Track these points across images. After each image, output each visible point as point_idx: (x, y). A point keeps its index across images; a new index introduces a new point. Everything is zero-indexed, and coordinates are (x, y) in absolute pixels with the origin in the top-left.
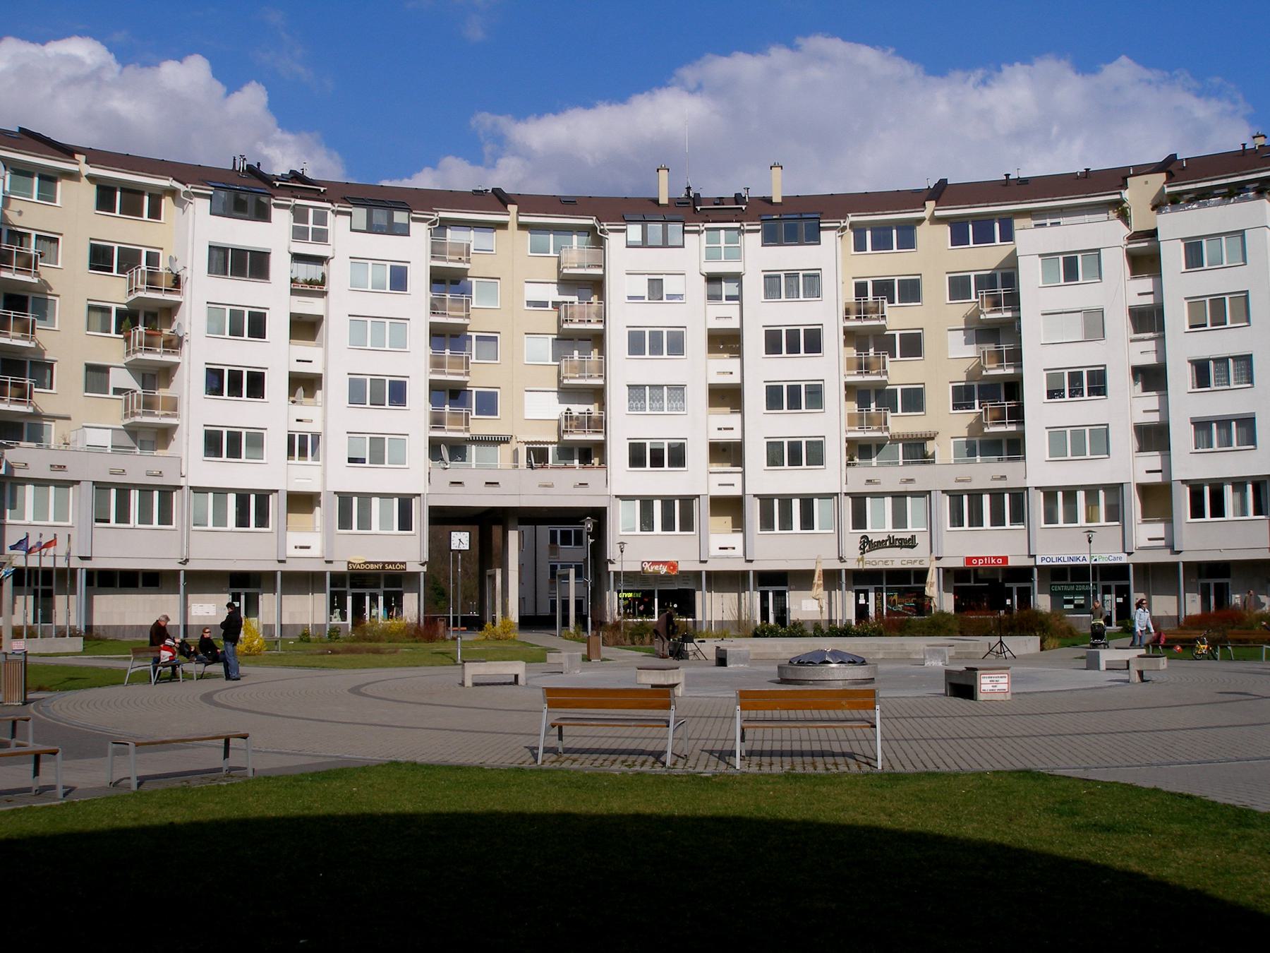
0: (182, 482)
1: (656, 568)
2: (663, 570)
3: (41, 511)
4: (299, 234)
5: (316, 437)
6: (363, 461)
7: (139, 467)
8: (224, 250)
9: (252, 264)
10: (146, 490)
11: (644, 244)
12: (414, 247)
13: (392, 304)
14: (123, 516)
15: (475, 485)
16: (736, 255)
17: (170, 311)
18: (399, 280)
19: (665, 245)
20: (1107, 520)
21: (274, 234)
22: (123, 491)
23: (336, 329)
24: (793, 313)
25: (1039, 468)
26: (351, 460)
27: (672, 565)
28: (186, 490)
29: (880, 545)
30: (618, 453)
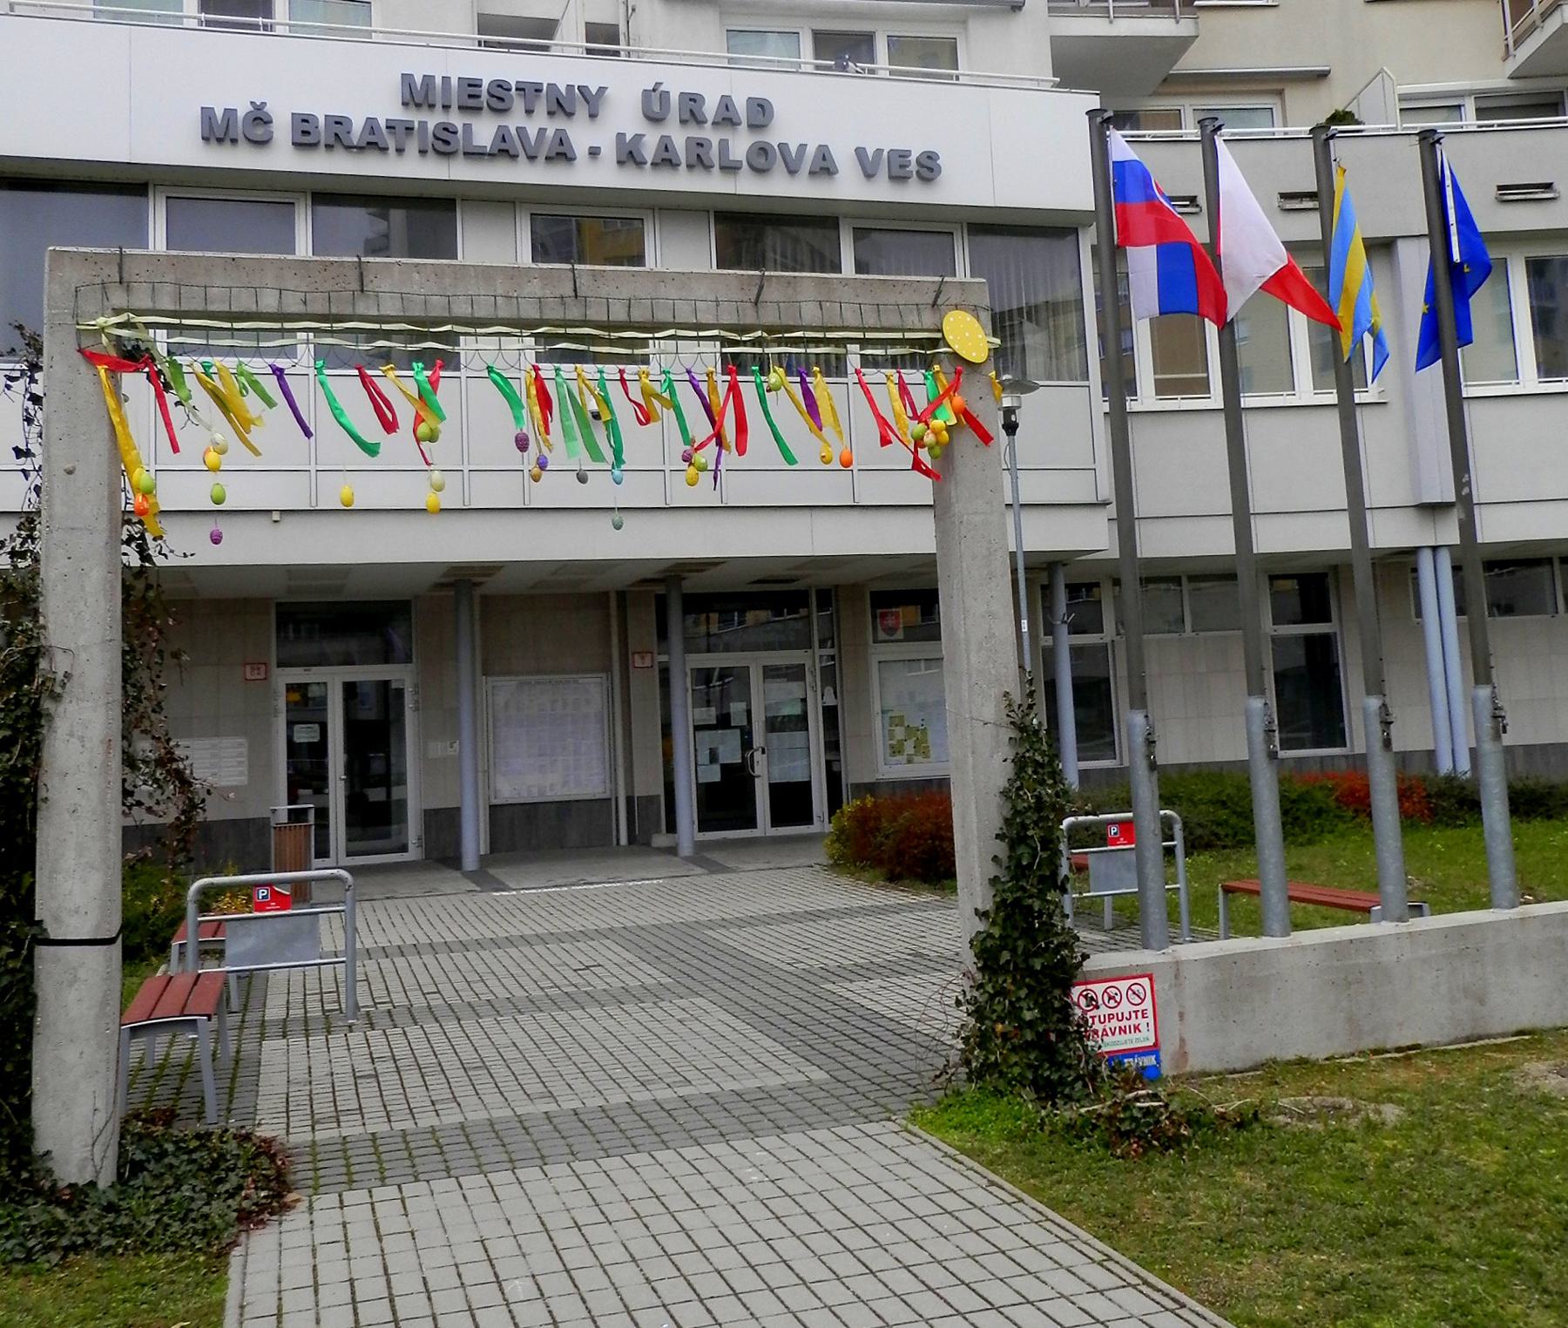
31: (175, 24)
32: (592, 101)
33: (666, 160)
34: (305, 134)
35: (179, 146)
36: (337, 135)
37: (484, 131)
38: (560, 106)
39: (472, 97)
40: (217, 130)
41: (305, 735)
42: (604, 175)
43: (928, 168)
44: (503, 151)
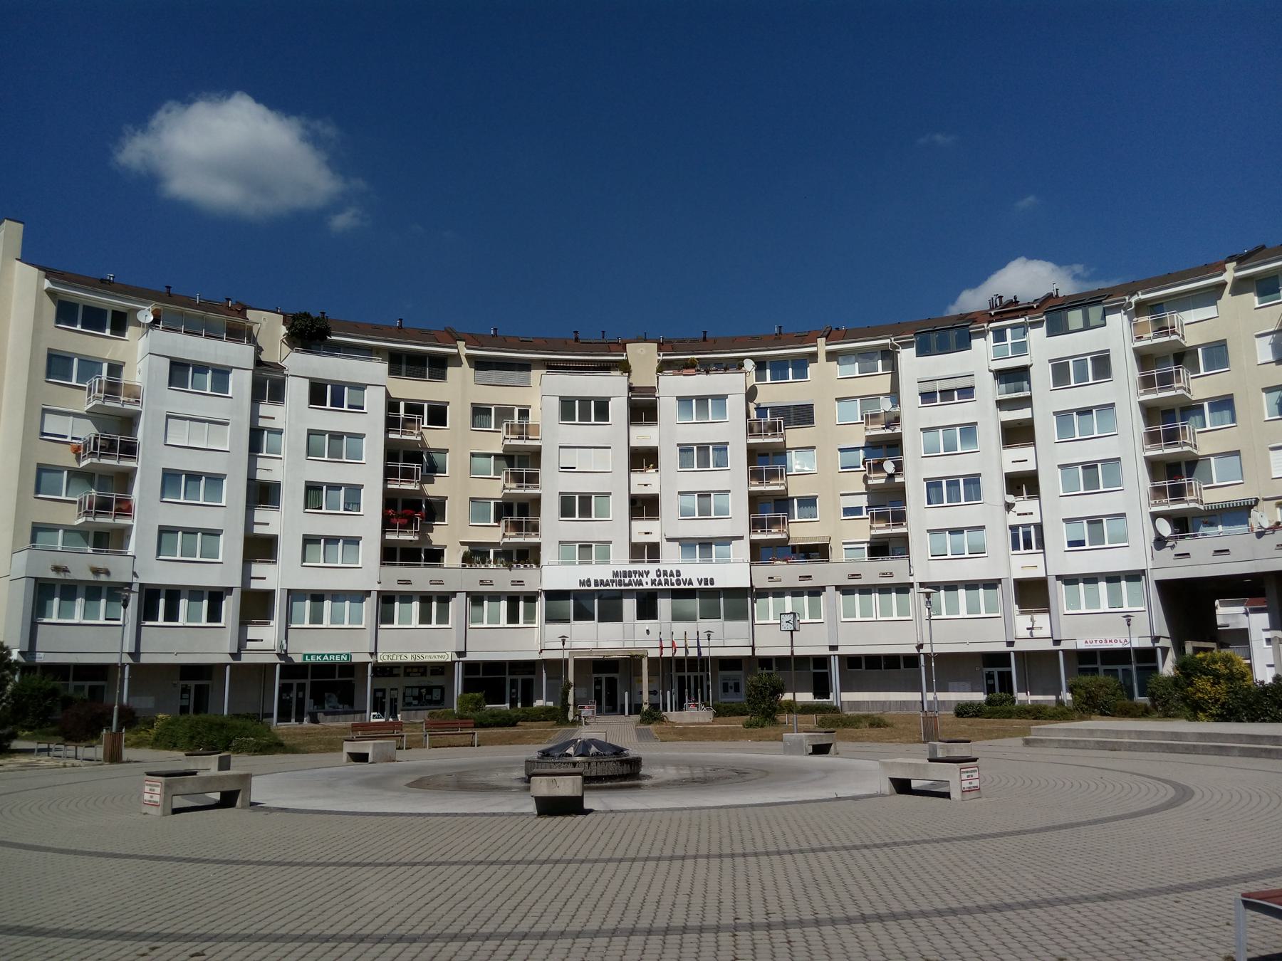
0: (911, 580)
5: (1039, 527)
6: (1082, 543)
7: (873, 571)
20: (208, 621)
23: (1046, 428)
26: (1071, 544)
28: (916, 586)
31: (574, 564)
32: (647, 573)
33: (660, 583)
34: (596, 584)
35: (577, 587)
36: (602, 582)
37: (627, 580)
38: (641, 574)
39: (625, 574)
40: (582, 583)
41: (598, 687)
42: (649, 586)
43: (712, 582)
44: (630, 584)
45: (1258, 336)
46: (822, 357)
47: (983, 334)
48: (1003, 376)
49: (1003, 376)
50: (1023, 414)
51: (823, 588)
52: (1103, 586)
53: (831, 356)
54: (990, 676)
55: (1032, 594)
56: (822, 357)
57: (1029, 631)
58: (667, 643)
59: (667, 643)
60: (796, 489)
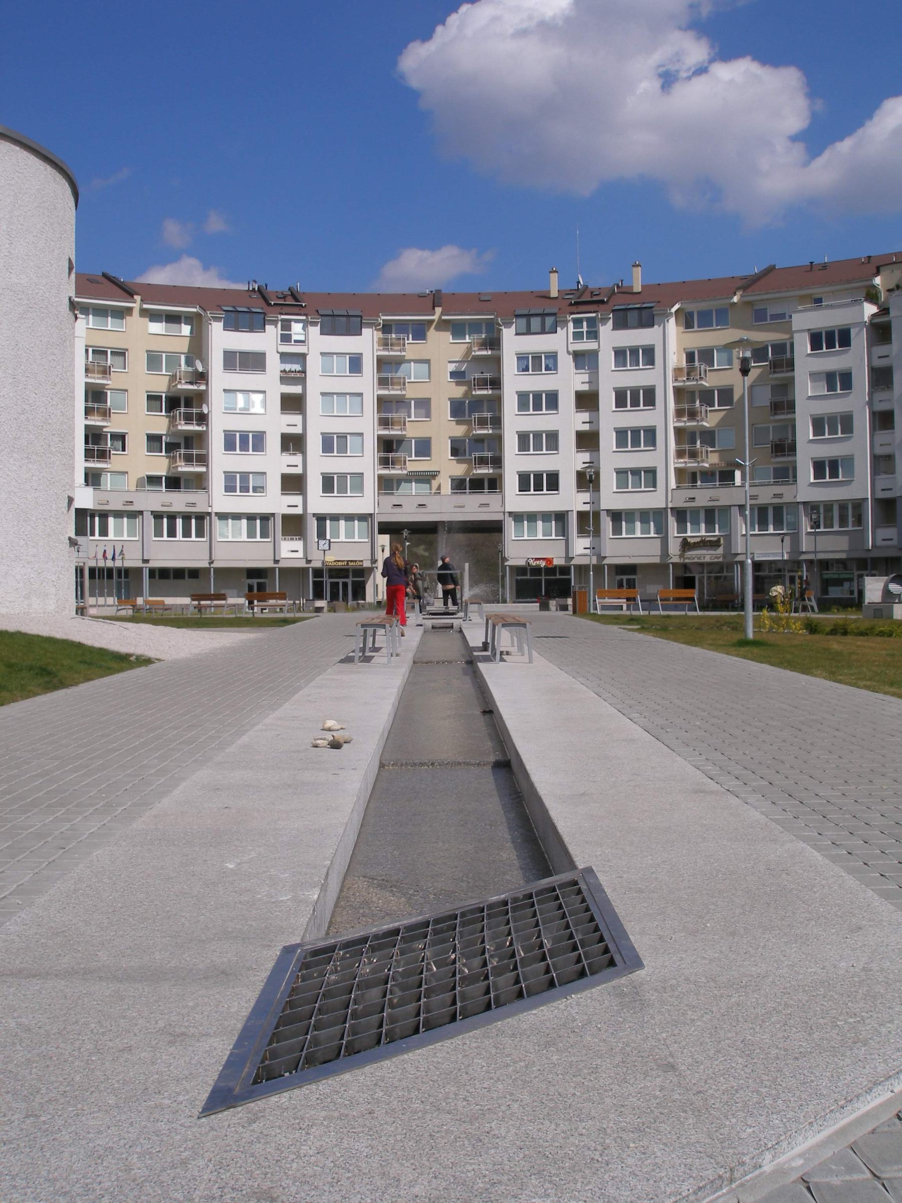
1: (538, 562)
2: (543, 564)
3: (119, 532)
4: (286, 339)
8: (234, 353)
9: (252, 362)
10: (187, 517)
11: (528, 332)
12: (366, 343)
13: (352, 384)
14: (172, 533)
15: (411, 506)
16: (594, 335)
17: (201, 397)
18: (356, 364)
19: (543, 332)
21: (265, 341)
22: (172, 517)
23: (314, 403)
24: (637, 377)
25: (806, 487)
27: (549, 561)
29: (696, 546)
30: (511, 482)
45: (450, 362)
46: (136, 312)
47: (274, 323)
48: (285, 357)
49: (285, 357)
50: (297, 389)
51: (141, 513)
52: (342, 523)
53: (144, 313)
54: (251, 588)
55: (294, 525)
56: (136, 312)
57: (291, 552)
58: (109, 555)
59: (109, 555)
60: (112, 426)
